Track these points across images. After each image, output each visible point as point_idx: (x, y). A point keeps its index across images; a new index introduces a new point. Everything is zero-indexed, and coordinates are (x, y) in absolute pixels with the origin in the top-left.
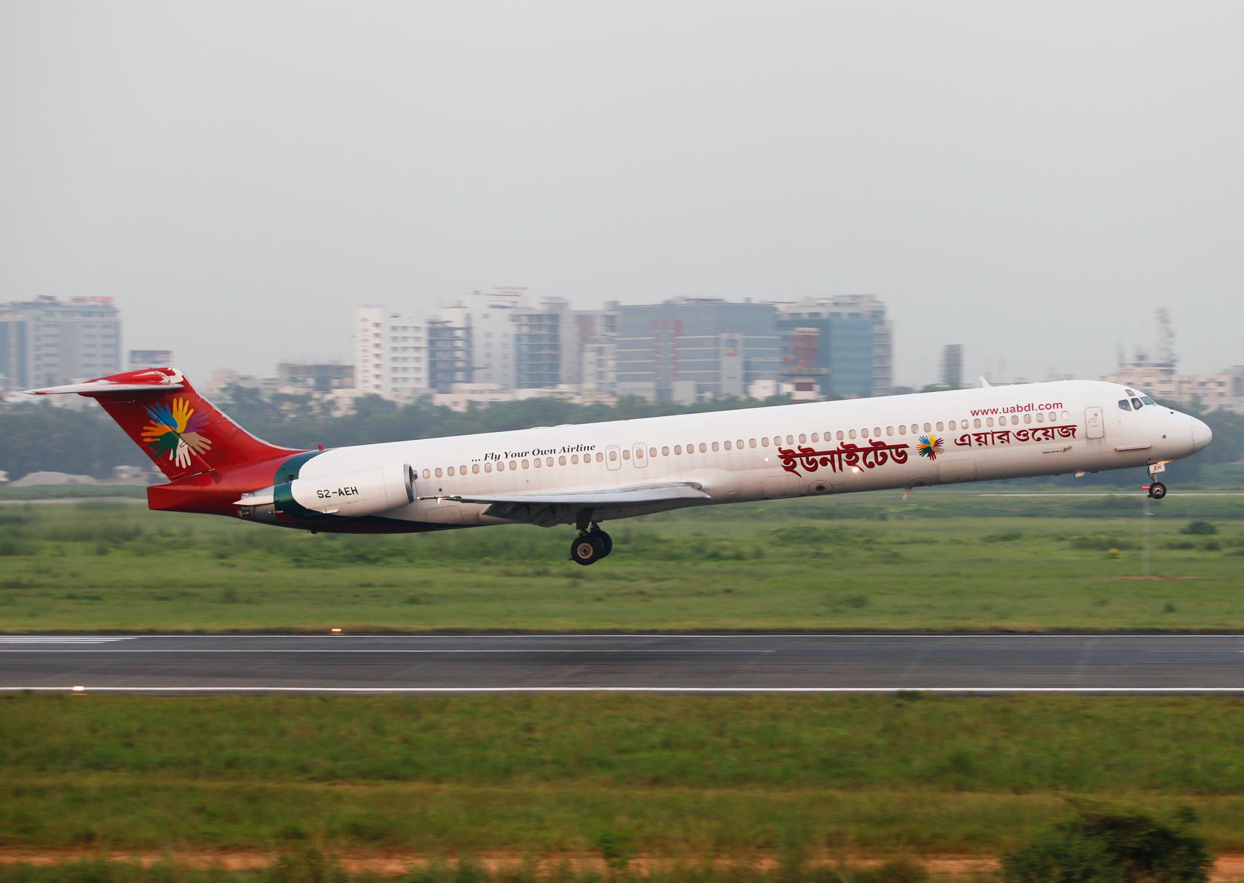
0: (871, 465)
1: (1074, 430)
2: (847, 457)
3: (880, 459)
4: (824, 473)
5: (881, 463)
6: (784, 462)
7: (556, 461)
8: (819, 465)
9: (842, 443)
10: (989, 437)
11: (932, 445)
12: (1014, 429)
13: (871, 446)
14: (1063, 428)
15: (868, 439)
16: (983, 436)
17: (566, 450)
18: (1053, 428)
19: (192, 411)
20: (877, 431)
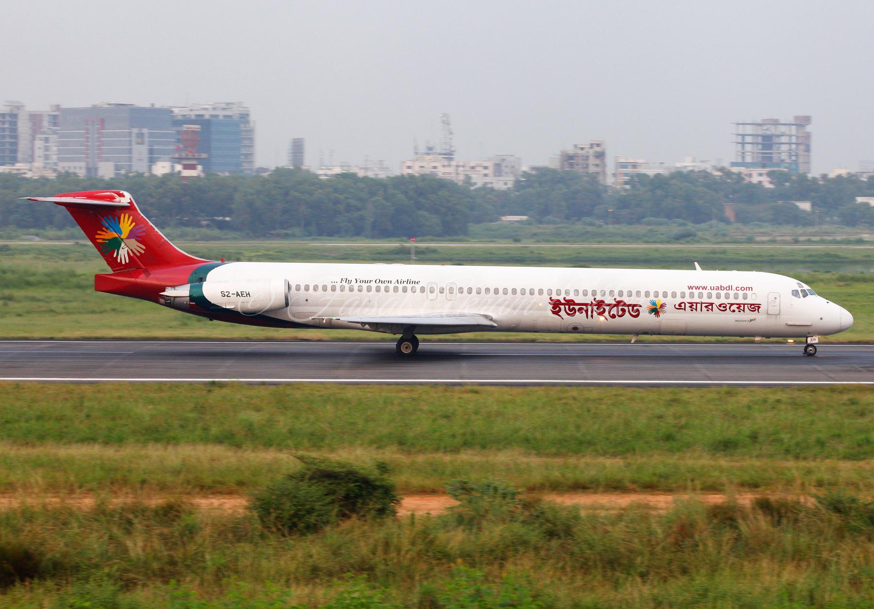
0: (613, 316)
1: (759, 307)
2: (597, 309)
3: (620, 313)
4: (579, 318)
5: (620, 316)
6: (553, 308)
7: (391, 289)
9: (595, 299)
10: (699, 305)
12: (717, 302)
14: (752, 305)
16: (695, 304)
17: (399, 282)
18: (744, 304)
19: (134, 224)
20: (621, 293)
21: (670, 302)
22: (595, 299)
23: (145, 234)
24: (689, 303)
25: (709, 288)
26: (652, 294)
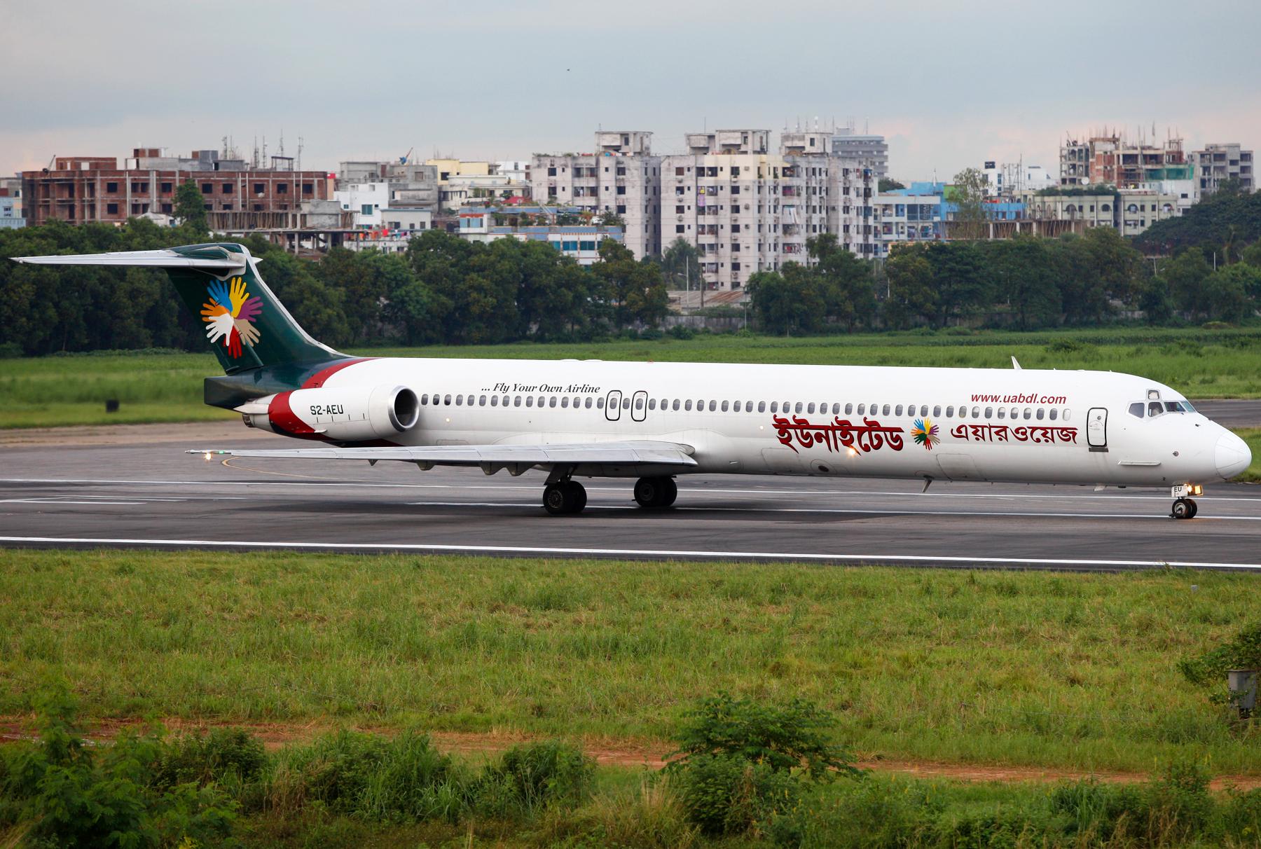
1: (1074, 434)
2: (843, 435)
3: (875, 442)
8: (815, 441)
9: (837, 418)
10: (986, 430)
11: (927, 432)
12: (1012, 424)
13: (865, 425)
14: (1063, 429)
15: (863, 417)
18: (1052, 429)
19: (247, 295)
21: (945, 425)
22: (837, 418)
23: (260, 312)
24: (972, 427)
25: (1002, 399)
26: (918, 412)
